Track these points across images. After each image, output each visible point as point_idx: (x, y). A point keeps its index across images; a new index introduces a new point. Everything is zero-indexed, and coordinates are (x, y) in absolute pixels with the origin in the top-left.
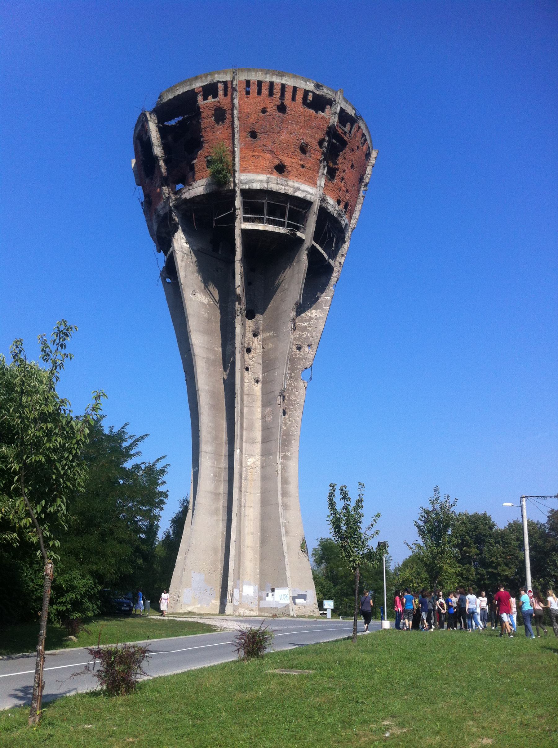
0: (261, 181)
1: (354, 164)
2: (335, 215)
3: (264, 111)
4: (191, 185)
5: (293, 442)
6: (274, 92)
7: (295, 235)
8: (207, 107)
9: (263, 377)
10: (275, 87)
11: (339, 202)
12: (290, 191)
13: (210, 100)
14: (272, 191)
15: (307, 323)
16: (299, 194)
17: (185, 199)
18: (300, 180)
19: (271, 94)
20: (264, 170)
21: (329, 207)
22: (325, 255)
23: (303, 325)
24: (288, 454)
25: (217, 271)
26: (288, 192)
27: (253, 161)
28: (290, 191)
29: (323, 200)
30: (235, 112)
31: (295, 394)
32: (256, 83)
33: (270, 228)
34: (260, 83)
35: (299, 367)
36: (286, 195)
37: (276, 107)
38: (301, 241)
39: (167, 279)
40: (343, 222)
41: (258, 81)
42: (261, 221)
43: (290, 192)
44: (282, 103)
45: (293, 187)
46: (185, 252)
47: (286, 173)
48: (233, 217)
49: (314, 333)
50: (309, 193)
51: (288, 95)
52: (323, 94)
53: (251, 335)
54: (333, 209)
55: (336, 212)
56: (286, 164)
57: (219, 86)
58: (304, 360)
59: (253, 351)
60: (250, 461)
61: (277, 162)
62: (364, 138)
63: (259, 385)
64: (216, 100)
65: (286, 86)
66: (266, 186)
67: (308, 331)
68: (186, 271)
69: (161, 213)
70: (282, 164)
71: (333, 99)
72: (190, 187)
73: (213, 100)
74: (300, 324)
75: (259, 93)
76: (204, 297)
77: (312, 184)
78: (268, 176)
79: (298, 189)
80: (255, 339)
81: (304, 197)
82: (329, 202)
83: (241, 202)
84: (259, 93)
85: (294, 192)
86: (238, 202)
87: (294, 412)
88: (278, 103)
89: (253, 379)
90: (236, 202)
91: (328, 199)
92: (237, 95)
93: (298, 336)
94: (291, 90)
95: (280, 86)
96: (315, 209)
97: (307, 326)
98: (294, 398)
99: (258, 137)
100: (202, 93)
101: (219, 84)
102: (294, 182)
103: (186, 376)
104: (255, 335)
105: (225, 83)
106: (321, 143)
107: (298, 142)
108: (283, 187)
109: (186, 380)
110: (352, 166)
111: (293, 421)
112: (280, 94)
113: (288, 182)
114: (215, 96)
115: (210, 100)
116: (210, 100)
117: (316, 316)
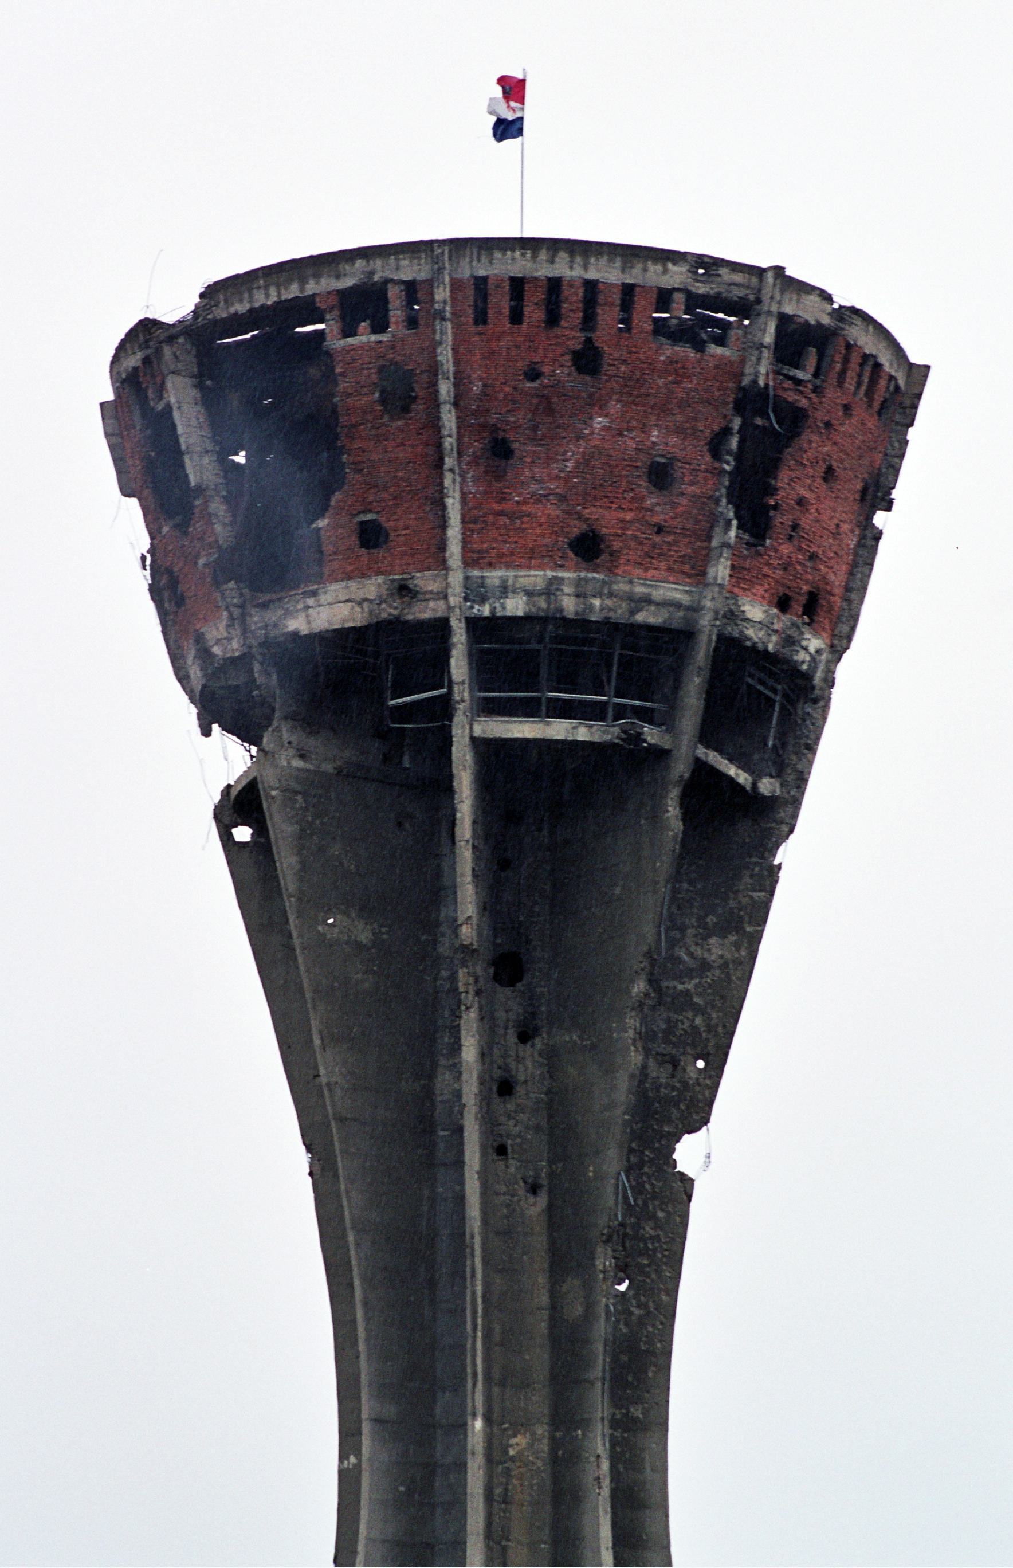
0: (529, 593)
1: (835, 464)
2: (771, 648)
3: (533, 374)
4: (314, 594)
5: (650, 1374)
6: (563, 311)
7: (638, 738)
8: (354, 360)
9: (552, 1175)
10: (566, 291)
11: (783, 604)
12: (619, 611)
13: (365, 337)
14: (564, 619)
15: (694, 982)
16: (644, 617)
17: (295, 635)
18: (651, 573)
19: (553, 318)
20: (533, 557)
21: (750, 632)
22: (743, 778)
23: (680, 987)
24: (637, 1412)
25: (400, 824)
26: (611, 614)
27: (503, 531)
28: (619, 611)
29: (733, 616)
30: (445, 389)
31: (654, 1217)
32: (507, 286)
33: (559, 729)
34: (518, 285)
35: (666, 1129)
36: (611, 627)
37: (568, 357)
38: (660, 755)
39: (234, 831)
40: (802, 656)
41: (512, 279)
42: (529, 709)
43: (620, 613)
44: (589, 341)
45: (630, 598)
46: (298, 788)
47: (604, 558)
48: (444, 708)
49: (714, 1015)
50: (677, 605)
51: (608, 317)
52: (722, 289)
53: (512, 1038)
54: (761, 634)
55: (774, 638)
56: (605, 531)
57: (390, 294)
58: (682, 1107)
59: (520, 1090)
60: (519, 1442)
61: (577, 528)
62: (868, 369)
63: (542, 1200)
64: (384, 337)
65: (601, 286)
66: (543, 605)
67: (698, 1010)
68: (300, 850)
69: (216, 650)
70: (593, 531)
71: (752, 297)
72: (311, 601)
73: (374, 338)
74: (672, 983)
75: (516, 317)
76: (360, 925)
77: (689, 576)
78: (550, 573)
79: (647, 600)
80: (526, 1050)
81: (665, 622)
82: (749, 616)
83: (470, 655)
84: (516, 317)
85: (633, 613)
86: (459, 667)
87: (654, 1276)
88: (575, 339)
89: (522, 1184)
90: (453, 662)
91: (746, 608)
92: (446, 332)
93: (663, 1026)
94: (617, 298)
95: (581, 292)
96: (702, 653)
97: (693, 991)
98: (652, 1232)
99: (517, 453)
100: (336, 312)
101: (390, 286)
102: (631, 582)
103: (311, 1167)
104: (524, 1037)
105: (411, 288)
106: (716, 446)
107: (642, 456)
108: (597, 602)
109: (311, 1174)
110: (829, 474)
111: (651, 1304)
112: (581, 315)
113: (615, 587)
114: (380, 326)
115: (364, 339)
116: (364, 339)
117: (722, 957)
